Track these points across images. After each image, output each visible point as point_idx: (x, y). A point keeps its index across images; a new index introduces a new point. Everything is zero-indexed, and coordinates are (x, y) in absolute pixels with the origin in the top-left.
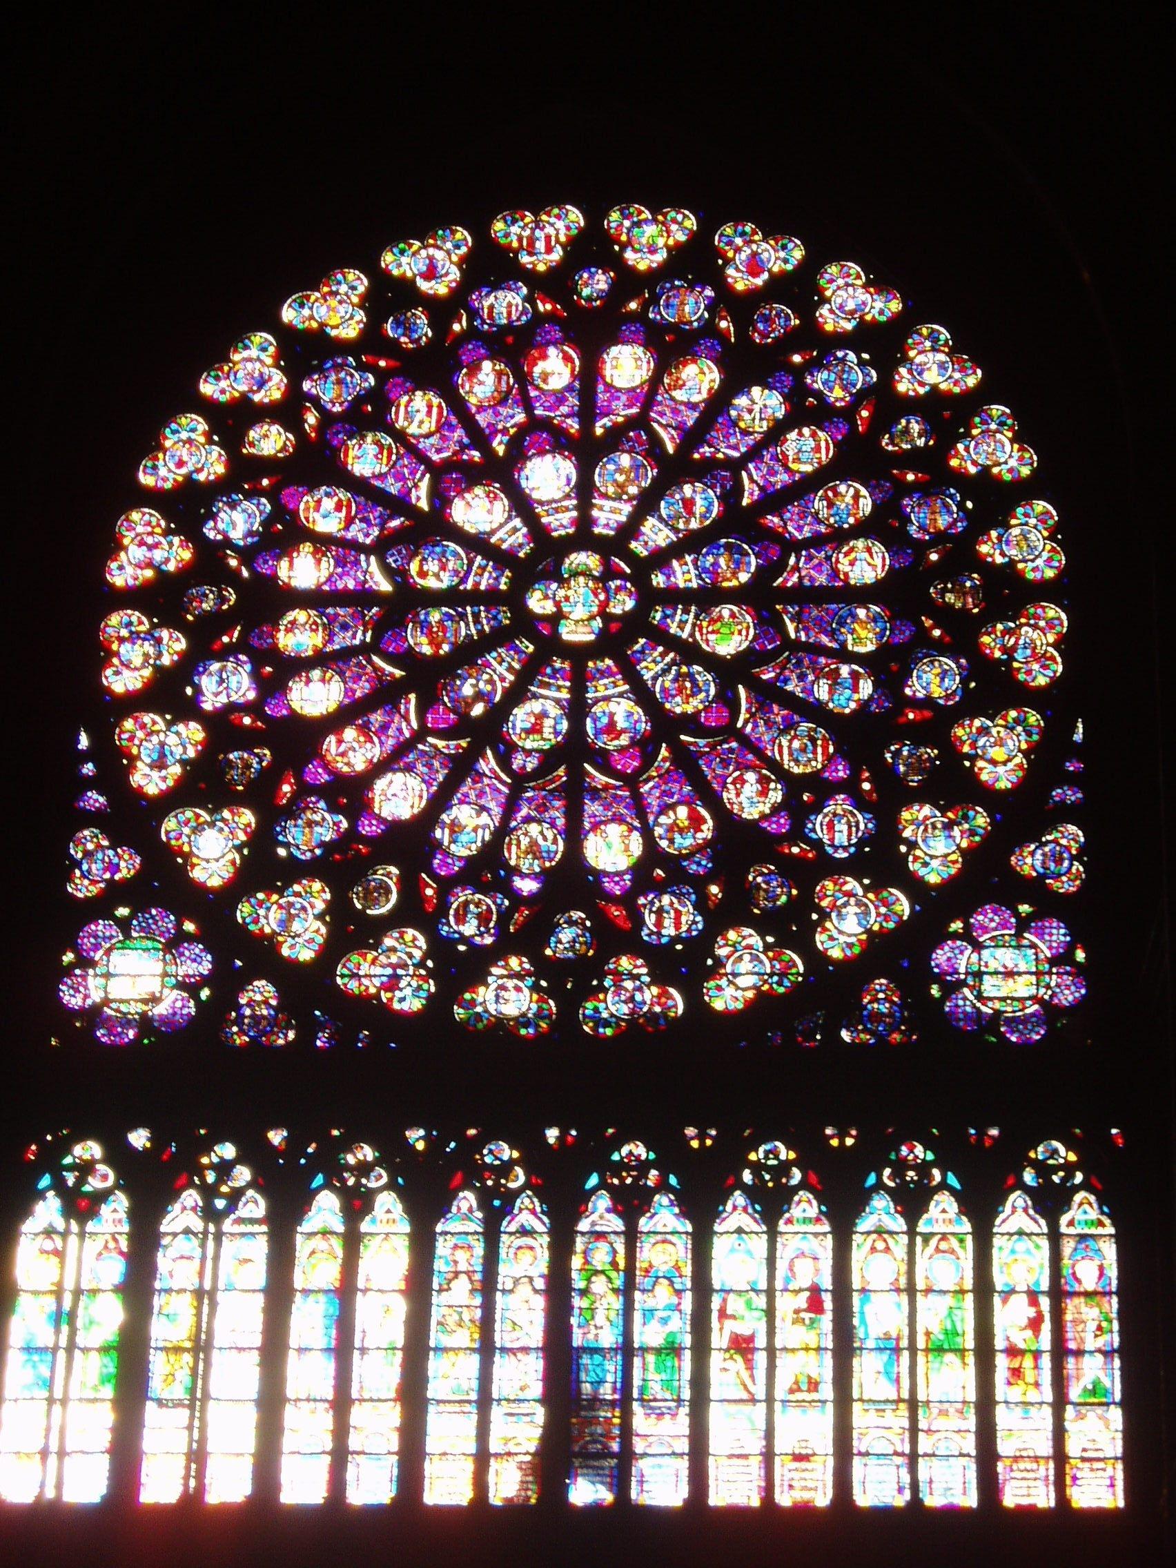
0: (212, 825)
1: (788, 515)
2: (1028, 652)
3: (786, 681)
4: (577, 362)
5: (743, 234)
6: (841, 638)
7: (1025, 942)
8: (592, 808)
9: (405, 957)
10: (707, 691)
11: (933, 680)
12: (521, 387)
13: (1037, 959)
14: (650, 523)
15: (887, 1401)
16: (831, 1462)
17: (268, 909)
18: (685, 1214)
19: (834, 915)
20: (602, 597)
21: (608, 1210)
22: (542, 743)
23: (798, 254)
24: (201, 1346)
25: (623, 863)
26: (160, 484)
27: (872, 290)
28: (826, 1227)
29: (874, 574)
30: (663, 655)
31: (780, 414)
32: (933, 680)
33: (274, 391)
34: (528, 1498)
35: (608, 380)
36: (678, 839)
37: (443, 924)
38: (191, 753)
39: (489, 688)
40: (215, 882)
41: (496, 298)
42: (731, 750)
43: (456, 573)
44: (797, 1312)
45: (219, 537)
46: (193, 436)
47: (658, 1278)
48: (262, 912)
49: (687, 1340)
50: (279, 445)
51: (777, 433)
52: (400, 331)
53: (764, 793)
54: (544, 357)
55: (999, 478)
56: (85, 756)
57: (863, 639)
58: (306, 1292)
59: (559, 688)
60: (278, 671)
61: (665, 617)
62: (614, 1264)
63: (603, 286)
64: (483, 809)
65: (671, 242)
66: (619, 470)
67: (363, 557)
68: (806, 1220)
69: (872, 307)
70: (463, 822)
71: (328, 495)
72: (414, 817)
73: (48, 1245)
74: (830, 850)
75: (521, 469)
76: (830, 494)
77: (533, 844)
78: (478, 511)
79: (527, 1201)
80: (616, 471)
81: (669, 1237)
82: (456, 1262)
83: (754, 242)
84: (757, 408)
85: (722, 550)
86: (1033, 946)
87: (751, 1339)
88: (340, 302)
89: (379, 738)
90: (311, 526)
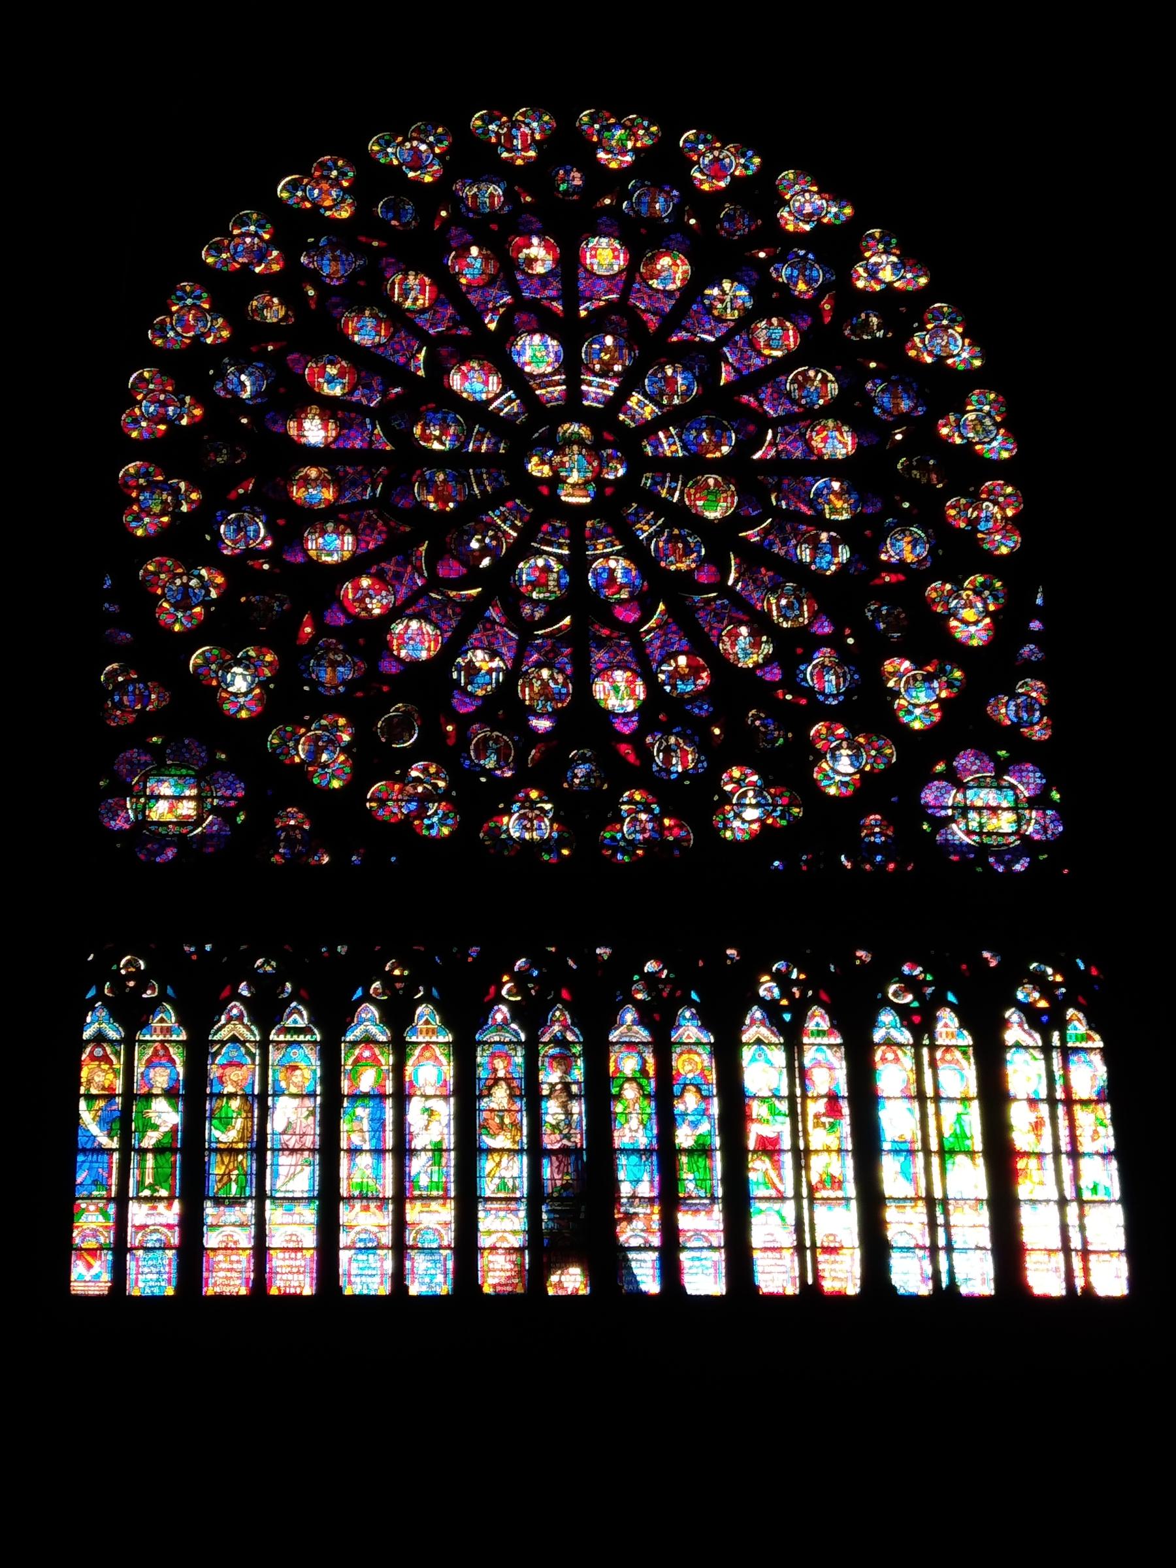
0: (238, 663)
1: (762, 396)
2: (991, 524)
3: (771, 544)
4: (558, 250)
5: (705, 141)
6: (819, 507)
7: (1004, 784)
8: (599, 656)
9: (429, 787)
10: (699, 552)
11: (904, 549)
12: (508, 270)
13: (1017, 799)
14: (634, 400)
15: (906, 1199)
16: (858, 1254)
17: (297, 742)
18: (706, 1026)
19: (828, 756)
20: (595, 464)
21: (634, 1022)
22: (548, 595)
23: (757, 160)
24: (259, 1146)
25: (631, 706)
26: (169, 345)
27: (827, 196)
28: (839, 1040)
29: (844, 451)
30: (656, 518)
31: (749, 305)
32: (904, 549)
33: (274, 263)
34: (577, 1290)
35: (589, 267)
36: (681, 686)
37: (465, 759)
38: (214, 594)
39: (494, 543)
40: (244, 714)
41: (479, 190)
42: (723, 606)
43: (456, 437)
44: (817, 1116)
45: (229, 396)
46: (198, 303)
47: (685, 1085)
48: (291, 744)
49: (717, 1142)
50: (282, 313)
51: (747, 320)
52: (390, 215)
53: (756, 645)
54: (529, 245)
55: (952, 369)
56: (110, 596)
57: (840, 510)
58: (355, 1097)
59: (560, 546)
60: (294, 523)
61: (655, 483)
62: (643, 1071)
63: (578, 182)
64: (494, 654)
65: (639, 145)
66: (604, 349)
67: (368, 421)
68: (820, 1033)
69: (828, 212)
70: (477, 664)
71: (333, 363)
72: (429, 661)
73: (98, 1052)
74: (821, 698)
75: (512, 345)
76: (800, 378)
77: (545, 685)
78: (473, 383)
79: (558, 1013)
80: (601, 350)
81: (694, 1048)
82: (495, 1070)
83: (717, 149)
84: (728, 298)
85: (704, 425)
86: (1012, 787)
87: (776, 1141)
88: (332, 186)
89: (393, 586)
90: (317, 390)
